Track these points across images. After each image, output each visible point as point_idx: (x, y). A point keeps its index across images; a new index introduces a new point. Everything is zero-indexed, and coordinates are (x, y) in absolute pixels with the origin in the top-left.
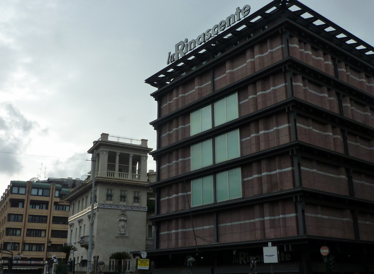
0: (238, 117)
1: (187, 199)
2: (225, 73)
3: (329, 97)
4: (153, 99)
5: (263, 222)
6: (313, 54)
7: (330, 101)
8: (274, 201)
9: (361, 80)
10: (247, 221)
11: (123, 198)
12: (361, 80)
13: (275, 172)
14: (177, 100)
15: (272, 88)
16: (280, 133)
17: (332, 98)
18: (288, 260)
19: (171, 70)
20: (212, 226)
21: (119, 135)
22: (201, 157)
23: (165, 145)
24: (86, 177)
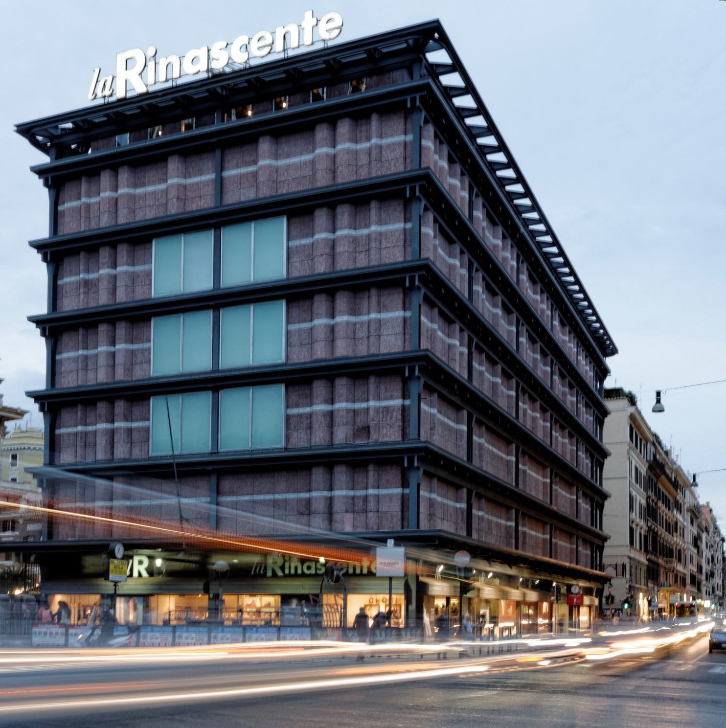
0: (284, 275)
2: (255, 162)
5: (330, 501)
8: (359, 461)
10: (292, 496)
16: (384, 326)
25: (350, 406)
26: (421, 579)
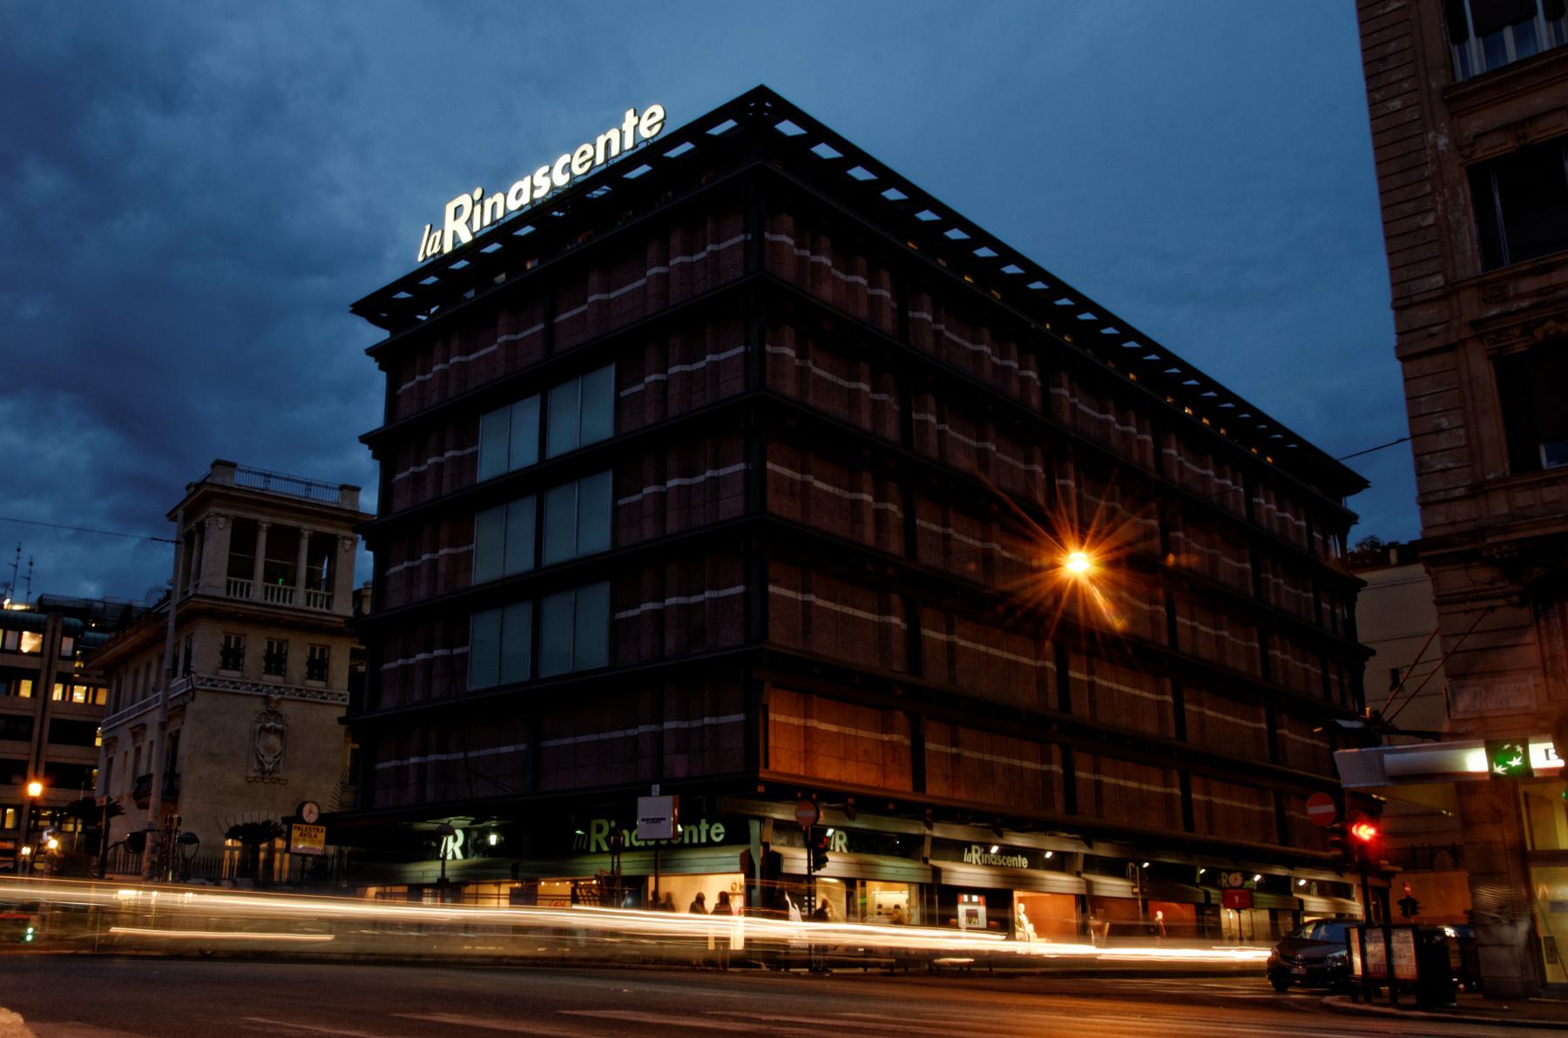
1: (457, 668)
2: (585, 301)
3: (874, 390)
4: (372, 364)
6: (835, 266)
7: (875, 403)
9: (977, 348)
10: (619, 734)
11: (275, 662)
12: (977, 348)
13: (699, 598)
14: (444, 375)
15: (709, 358)
17: (884, 397)
18: (718, 840)
19: (431, 280)
20: (523, 747)
21: (267, 467)
22: (501, 548)
23: (400, 504)
24: (161, 596)
25: (682, 600)
26: (773, 848)
